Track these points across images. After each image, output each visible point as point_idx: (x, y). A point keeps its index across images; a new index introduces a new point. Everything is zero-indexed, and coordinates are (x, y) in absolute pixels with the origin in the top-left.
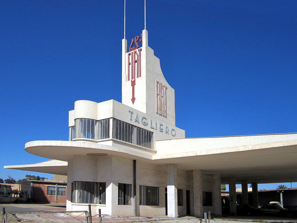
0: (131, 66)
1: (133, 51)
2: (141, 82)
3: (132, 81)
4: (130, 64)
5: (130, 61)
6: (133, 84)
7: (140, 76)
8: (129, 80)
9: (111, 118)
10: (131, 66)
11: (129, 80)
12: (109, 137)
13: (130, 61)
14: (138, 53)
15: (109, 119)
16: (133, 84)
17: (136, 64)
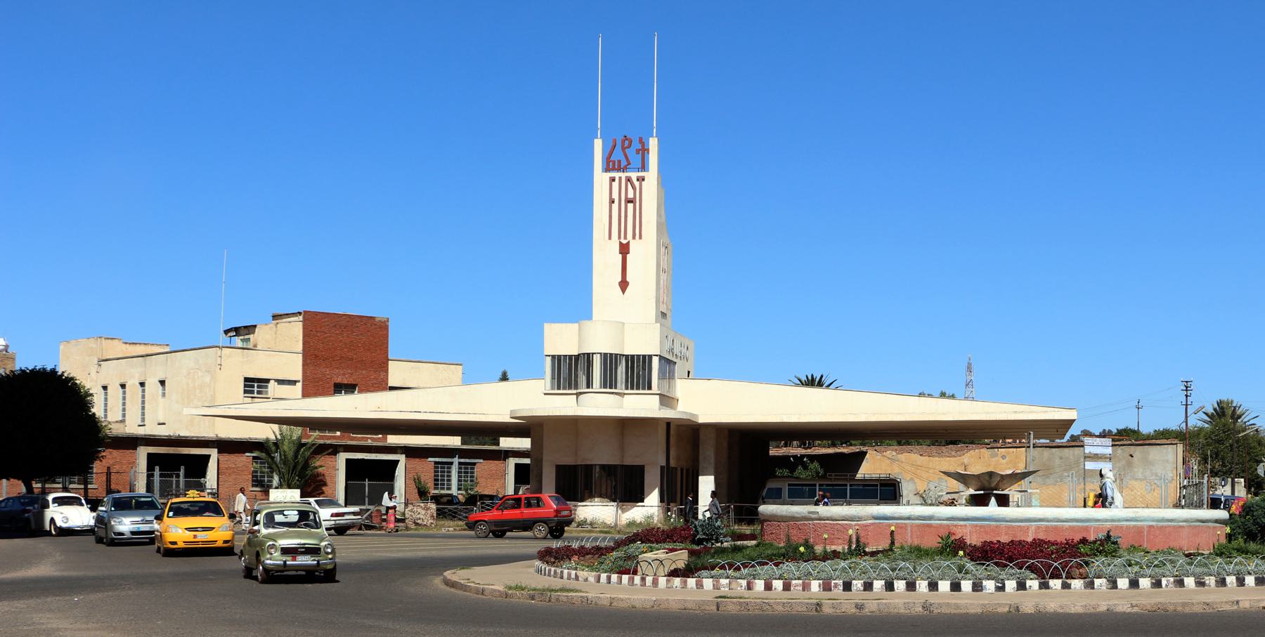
0: (615, 206)
1: (623, 175)
2: (645, 254)
3: (621, 244)
4: (613, 202)
5: (615, 196)
6: (624, 249)
7: (640, 238)
8: (610, 238)
9: (657, 355)
10: (615, 206)
11: (610, 238)
12: (650, 388)
13: (615, 196)
14: (637, 184)
15: (650, 357)
16: (624, 249)
17: (630, 206)
